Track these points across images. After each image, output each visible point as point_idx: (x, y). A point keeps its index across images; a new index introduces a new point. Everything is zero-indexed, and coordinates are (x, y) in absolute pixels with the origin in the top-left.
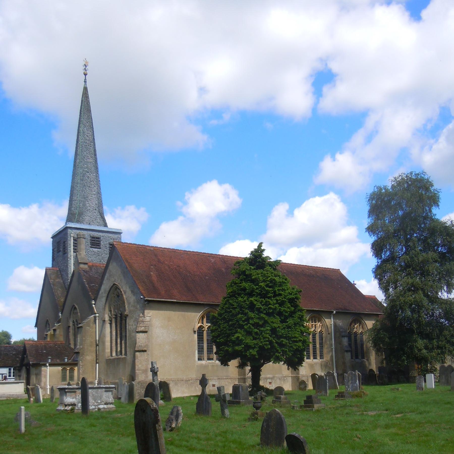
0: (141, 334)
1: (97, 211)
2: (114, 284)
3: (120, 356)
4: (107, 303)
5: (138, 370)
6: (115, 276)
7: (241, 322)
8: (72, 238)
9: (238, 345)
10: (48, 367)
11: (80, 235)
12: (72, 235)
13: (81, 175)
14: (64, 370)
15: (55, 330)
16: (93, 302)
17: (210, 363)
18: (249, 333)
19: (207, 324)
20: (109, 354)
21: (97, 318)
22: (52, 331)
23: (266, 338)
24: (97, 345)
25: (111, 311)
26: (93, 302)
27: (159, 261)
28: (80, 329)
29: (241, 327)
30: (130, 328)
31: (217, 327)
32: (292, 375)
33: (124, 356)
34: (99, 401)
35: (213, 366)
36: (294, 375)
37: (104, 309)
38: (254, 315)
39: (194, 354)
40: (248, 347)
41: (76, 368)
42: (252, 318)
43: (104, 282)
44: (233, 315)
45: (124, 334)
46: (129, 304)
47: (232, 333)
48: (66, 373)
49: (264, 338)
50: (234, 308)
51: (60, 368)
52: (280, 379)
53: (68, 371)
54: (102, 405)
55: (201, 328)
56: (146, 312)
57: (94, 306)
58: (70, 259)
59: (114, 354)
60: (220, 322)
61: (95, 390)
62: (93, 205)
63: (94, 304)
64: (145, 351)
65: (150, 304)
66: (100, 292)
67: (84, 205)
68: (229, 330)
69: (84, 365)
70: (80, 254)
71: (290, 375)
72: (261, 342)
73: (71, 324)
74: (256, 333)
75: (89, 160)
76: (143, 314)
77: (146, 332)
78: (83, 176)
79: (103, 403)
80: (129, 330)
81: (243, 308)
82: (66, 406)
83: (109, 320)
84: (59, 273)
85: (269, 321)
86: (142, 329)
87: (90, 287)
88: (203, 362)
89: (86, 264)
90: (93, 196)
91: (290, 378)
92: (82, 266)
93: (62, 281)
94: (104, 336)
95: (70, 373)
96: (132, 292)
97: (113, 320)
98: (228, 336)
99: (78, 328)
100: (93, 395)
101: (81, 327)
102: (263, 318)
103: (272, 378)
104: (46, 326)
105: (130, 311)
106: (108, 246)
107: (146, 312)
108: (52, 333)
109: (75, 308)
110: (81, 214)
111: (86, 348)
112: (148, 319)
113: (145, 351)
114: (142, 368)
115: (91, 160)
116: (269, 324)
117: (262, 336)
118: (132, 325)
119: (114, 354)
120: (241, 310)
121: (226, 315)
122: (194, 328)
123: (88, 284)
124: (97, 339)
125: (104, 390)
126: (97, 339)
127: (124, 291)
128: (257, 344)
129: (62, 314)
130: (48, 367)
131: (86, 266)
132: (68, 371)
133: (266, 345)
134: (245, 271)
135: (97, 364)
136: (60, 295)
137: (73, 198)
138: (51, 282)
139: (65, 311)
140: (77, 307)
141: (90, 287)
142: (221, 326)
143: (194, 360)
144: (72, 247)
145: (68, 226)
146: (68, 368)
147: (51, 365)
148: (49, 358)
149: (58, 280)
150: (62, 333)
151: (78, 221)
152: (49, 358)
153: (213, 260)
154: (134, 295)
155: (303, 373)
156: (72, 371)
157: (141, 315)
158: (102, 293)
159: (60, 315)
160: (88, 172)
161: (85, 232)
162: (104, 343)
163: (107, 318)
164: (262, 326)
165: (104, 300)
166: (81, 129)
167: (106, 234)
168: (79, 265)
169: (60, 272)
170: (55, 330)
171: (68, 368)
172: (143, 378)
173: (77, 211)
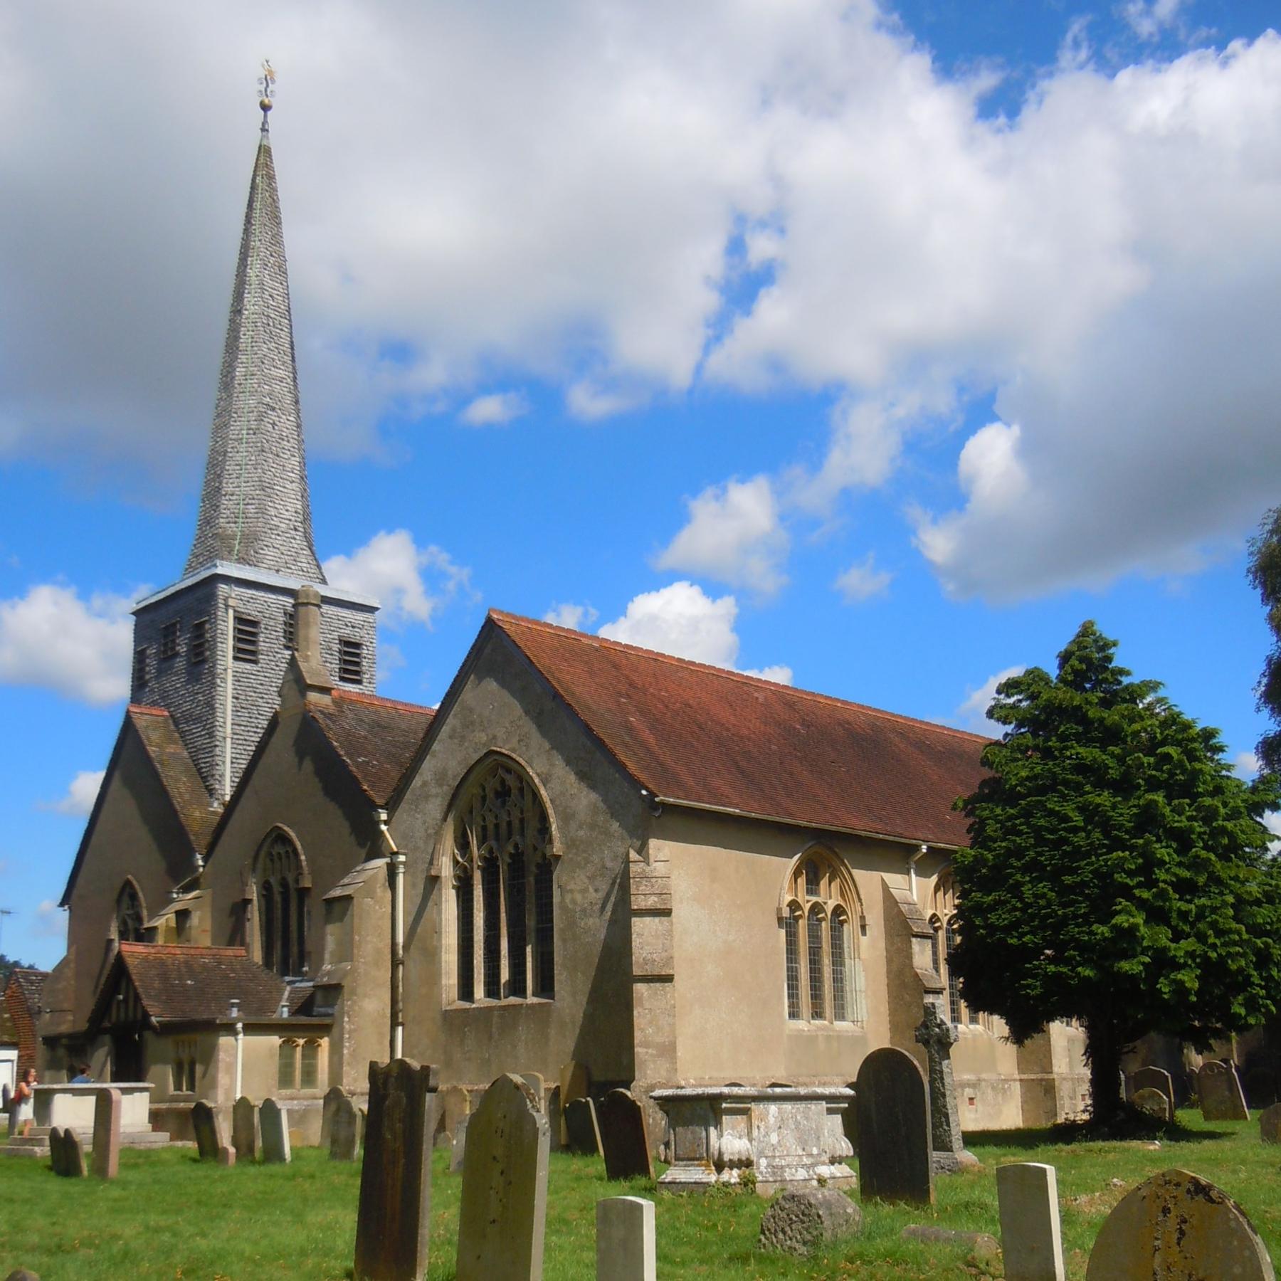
0: (648, 920)
1: (299, 535)
2: (491, 753)
3: (513, 1000)
4: (450, 819)
5: (646, 1045)
6: (501, 723)
7: (1120, 877)
8: (231, 612)
9: (1127, 955)
10: (241, 1036)
11: (307, 596)
12: (231, 602)
13: (252, 416)
14: (288, 1044)
15: (183, 915)
16: (384, 817)
17: (819, 1028)
18: (1157, 915)
19: (808, 898)
20: (454, 993)
21: (401, 869)
22: (173, 916)
23: (1230, 931)
24: (395, 963)
25: (463, 845)
26: (384, 817)
27: (631, 684)
28: (337, 908)
29: (1126, 892)
30: (574, 902)
31: (1004, 896)
32: (1025, 1077)
33: (531, 1000)
34: (815, 1151)
35: (828, 1038)
36: (1033, 1077)
37: (438, 835)
38: (1169, 854)
39: (781, 998)
40: (1163, 963)
41: (325, 1042)
42: (1162, 863)
43: (436, 746)
44: (1078, 854)
45: (531, 922)
46: (566, 818)
47: (1076, 917)
48: (292, 1056)
49: (1220, 933)
50: (1075, 830)
51: (276, 1040)
52: (993, 1088)
53: (299, 1050)
54: (824, 1164)
55: (794, 905)
56: (653, 843)
57: (384, 827)
58: (224, 680)
59: (479, 991)
60: (1018, 877)
61: (801, 1106)
62: (287, 515)
63: (386, 823)
64: (668, 979)
65: (658, 817)
66: (417, 782)
67: (262, 511)
68: (1064, 905)
69: (355, 1030)
70: (307, 658)
71: (1017, 1077)
72: (1214, 947)
73: (253, 893)
74: (1183, 915)
75: (275, 372)
76: (642, 850)
77: (666, 913)
78: (260, 419)
79: (825, 1158)
80: (563, 908)
81: (1114, 827)
82: (720, 1166)
83: (458, 878)
84: (172, 727)
85: (1223, 875)
86: (652, 902)
87: (358, 765)
88: (802, 1025)
89: (325, 690)
90: (289, 486)
91: (1018, 1084)
92: (313, 696)
93: (185, 754)
94: (437, 931)
95: (304, 1056)
96: (582, 776)
97: (477, 877)
98: (1063, 923)
99: (330, 902)
100: (797, 1123)
101: (349, 898)
102: (1198, 865)
103: (974, 1085)
104: (119, 901)
105: (571, 844)
106: (336, 647)
107: (653, 843)
108: (173, 924)
109: (284, 839)
110: (250, 539)
111: (361, 970)
112: (658, 868)
113: (668, 979)
114: (659, 1039)
115: (281, 373)
116: (1227, 886)
117: (1213, 925)
118: (584, 891)
119: (479, 991)
120: (1106, 834)
121: (1040, 854)
122: (779, 910)
123: (347, 754)
124: (400, 939)
125: (824, 1104)
126: (400, 939)
127: (538, 775)
128: (1191, 955)
129: (206, 859)
130: (241, 1036)
131: (325, 700)
132: (299, 1050)
133: (1229, 955)
134: (1079, 708)
135: (400, 1028)
136: (187, 797)
137: (219, 489)
138: (153, 755)
139: (218, 851)
140: (292, 834)
141: (357, 768)
142: (1027, 891)
143: (781, 1016)
144: (231, 642)
145: (220, 571)
146: (301, 1041)
147: (250, 1029)
148: (233, 1005)
149: (171, 749)
150: (208, 925)
151: (242, 560)
152: (233, 1005)
153: (760, 697)
154: (593, 787)
155: (1060, 1071)
156: (311, 1047)
157: (633, 855)
158: (425, 784)
159: (200, 863)
160: (273, 409)
161: (271, 597)
162: (432, 955)
163: (446, 869)
164: (1204, 891)
165: (434, 808)
166: (251, 273)
167: (333, 608)
168: (303, 695)
169: (176, 723)
170: (183, 915)
171: (301, 1041)
172: (663, 1073)
173: (232, 529)
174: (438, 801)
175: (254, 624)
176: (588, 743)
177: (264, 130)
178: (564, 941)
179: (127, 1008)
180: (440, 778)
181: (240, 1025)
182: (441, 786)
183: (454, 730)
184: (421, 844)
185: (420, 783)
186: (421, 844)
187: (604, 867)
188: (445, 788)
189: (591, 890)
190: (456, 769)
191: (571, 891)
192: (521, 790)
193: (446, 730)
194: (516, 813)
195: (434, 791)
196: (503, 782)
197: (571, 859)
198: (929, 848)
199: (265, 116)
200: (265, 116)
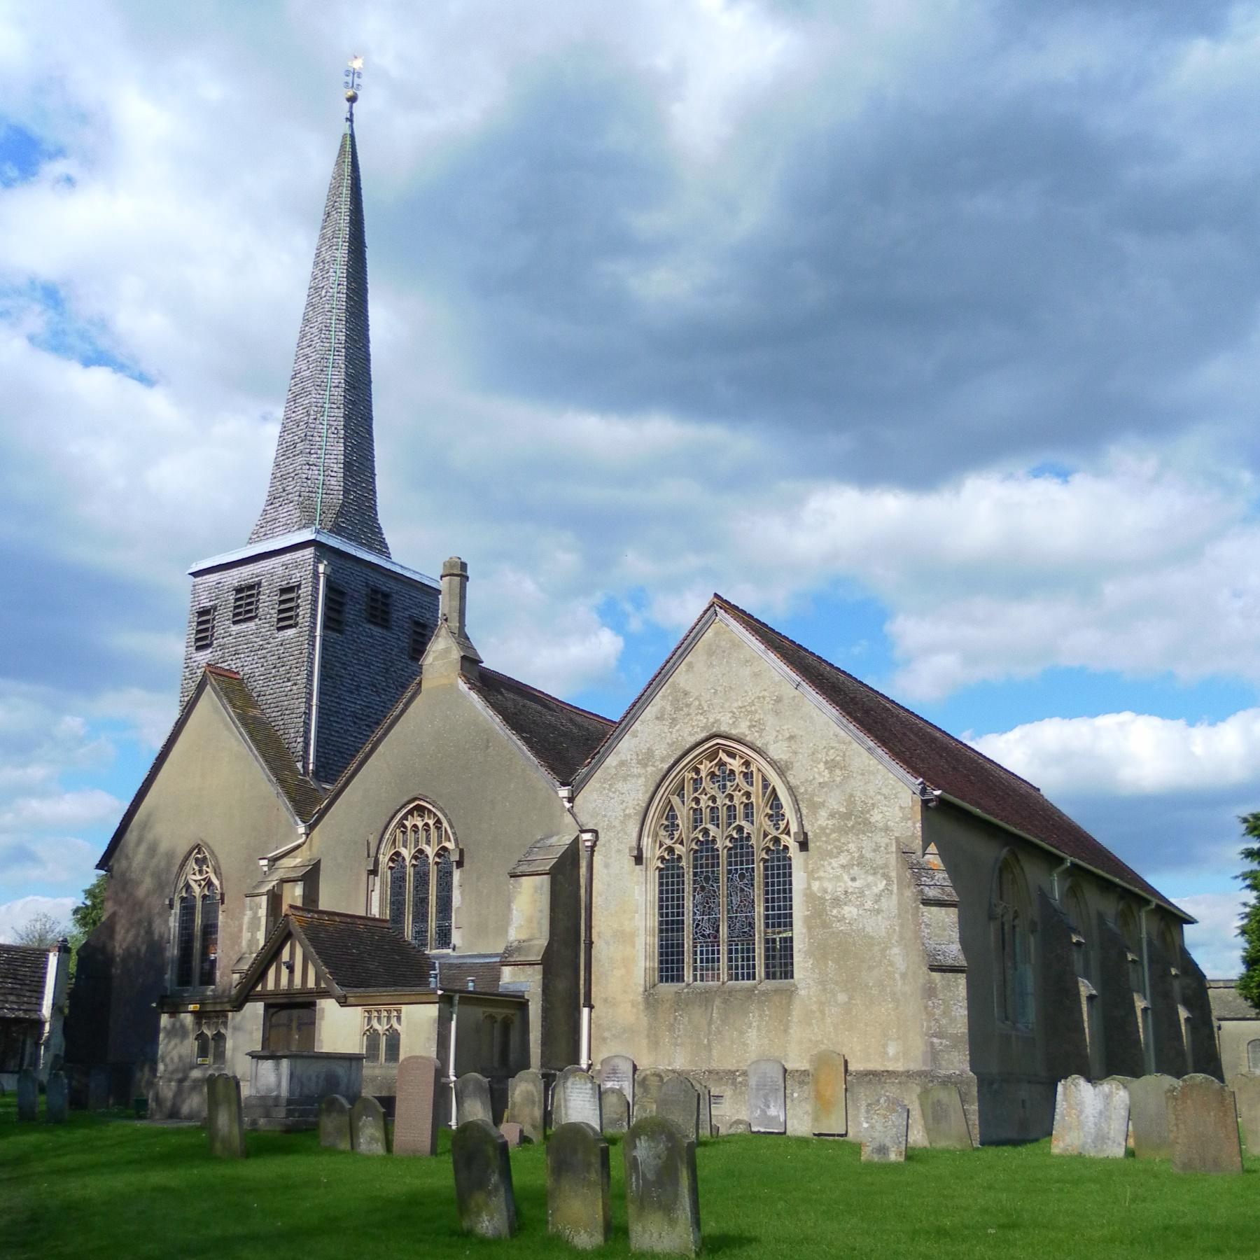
118: (839, 878)
158: (622, 763)
174: (641, 781)
175: (342, 594)
176: (842, 733)
177: (350, 120)
178: (810, 928)
179: (291, 968)
180: (646, 759)
181: (457, 997)
182: (645, 766)
183: (662, 711)
184: (616, 823)
185: (614, 764)
186: (616, 823)
187: (861, 856)
188: (650, 769)
189: (846, 877)
190: (663, 755)
191: (819, 879)
192: (748, 776)
193: (650, 712)
194: (738, 798)
195: (635, 771)
196: (722, 764)
197: (819, 847)
198: (1072, 863)
199: (351, 107)
200: (351, 107)
